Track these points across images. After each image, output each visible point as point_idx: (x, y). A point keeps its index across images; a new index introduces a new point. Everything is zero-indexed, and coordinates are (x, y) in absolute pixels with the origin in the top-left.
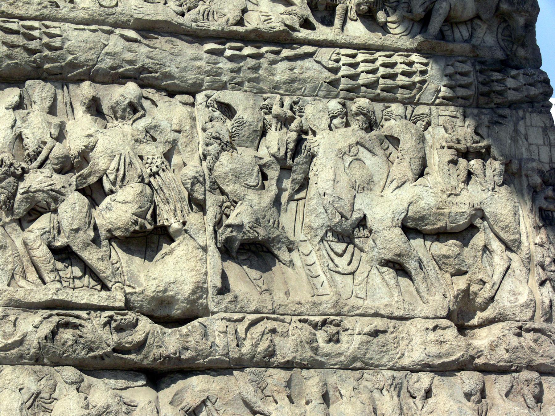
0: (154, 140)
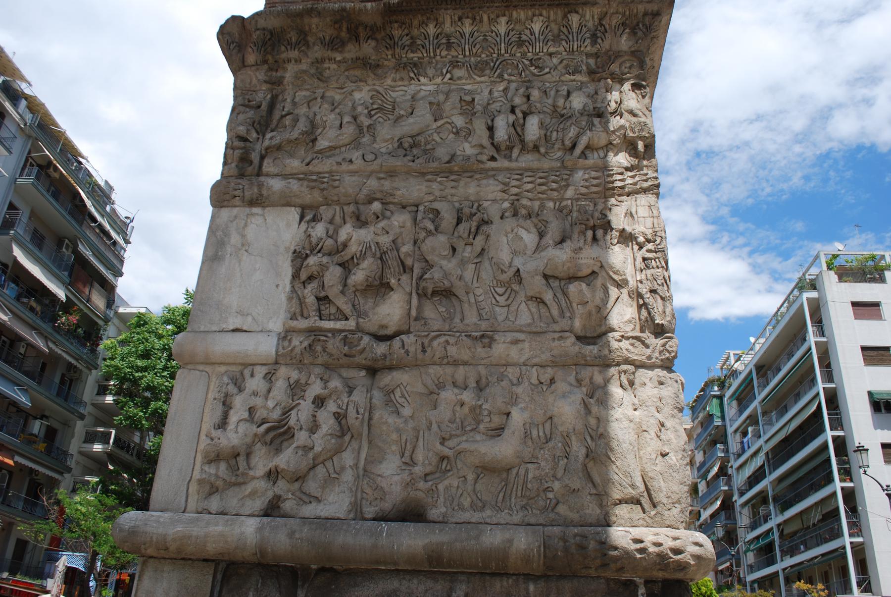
0: (388, 233)
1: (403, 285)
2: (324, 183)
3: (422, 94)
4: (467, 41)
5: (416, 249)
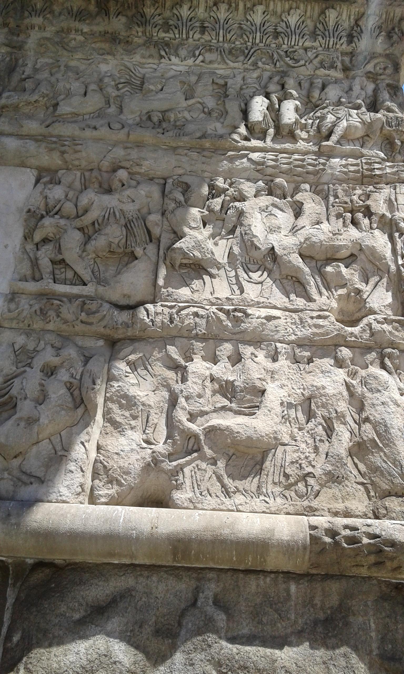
0: (133, 201)
1: (148, 254)
2: (64, 145)
3: (172, 73)
4: (221, 26)
5: (165, 219)
